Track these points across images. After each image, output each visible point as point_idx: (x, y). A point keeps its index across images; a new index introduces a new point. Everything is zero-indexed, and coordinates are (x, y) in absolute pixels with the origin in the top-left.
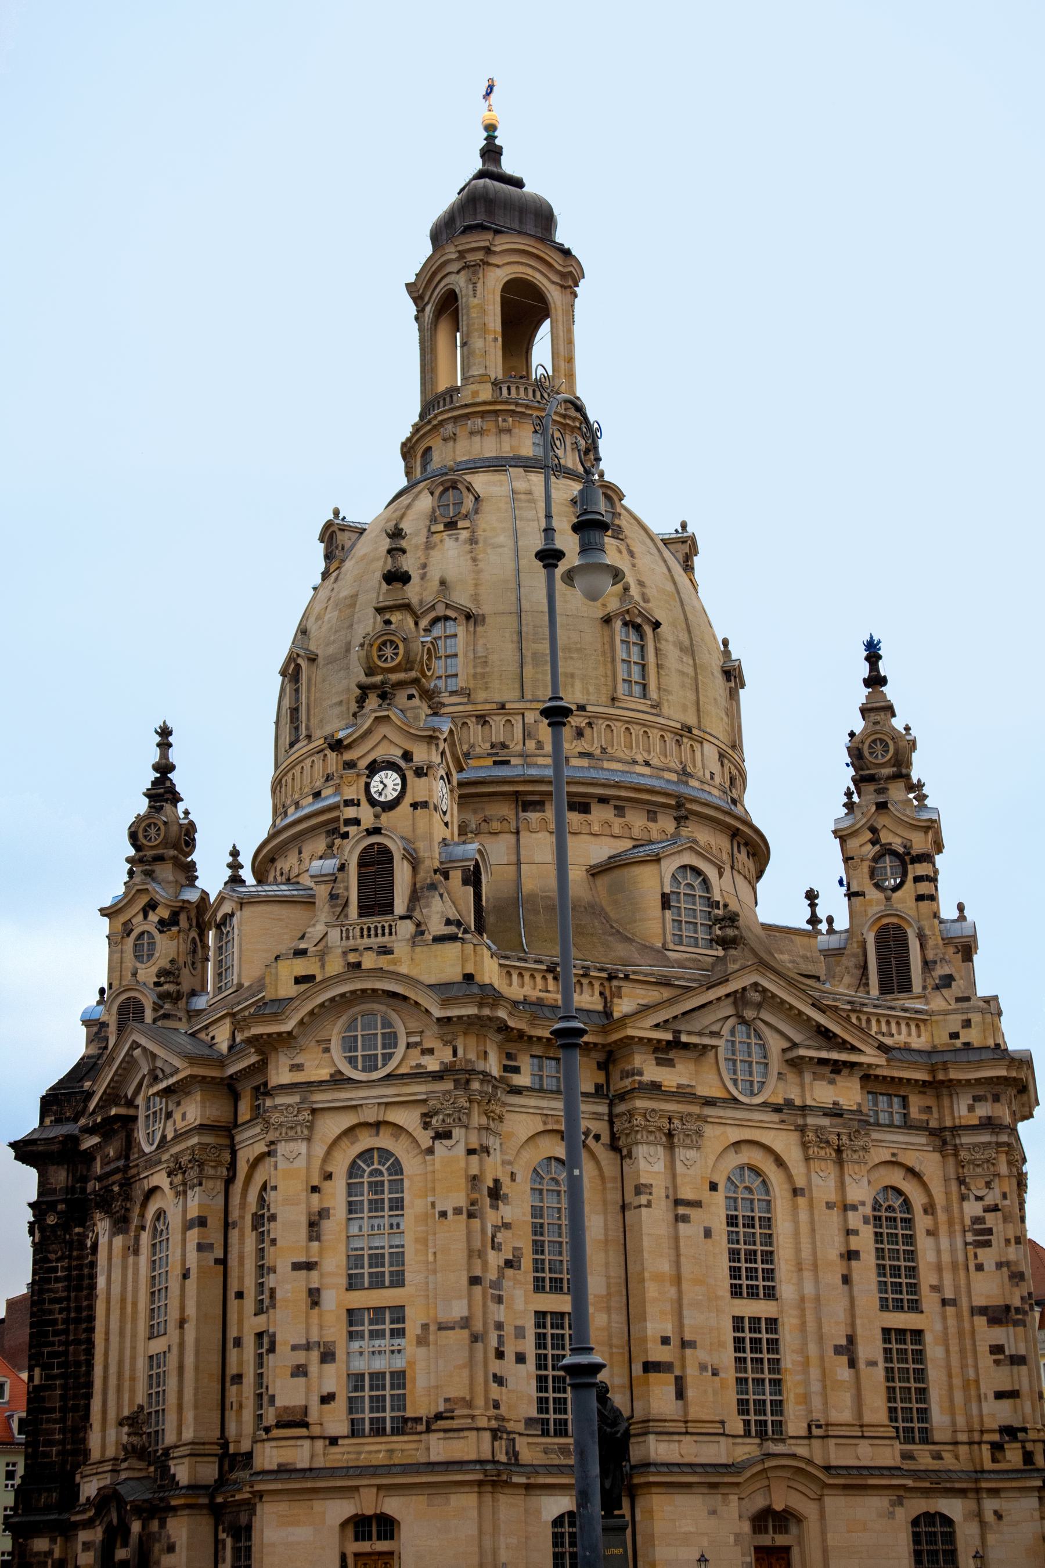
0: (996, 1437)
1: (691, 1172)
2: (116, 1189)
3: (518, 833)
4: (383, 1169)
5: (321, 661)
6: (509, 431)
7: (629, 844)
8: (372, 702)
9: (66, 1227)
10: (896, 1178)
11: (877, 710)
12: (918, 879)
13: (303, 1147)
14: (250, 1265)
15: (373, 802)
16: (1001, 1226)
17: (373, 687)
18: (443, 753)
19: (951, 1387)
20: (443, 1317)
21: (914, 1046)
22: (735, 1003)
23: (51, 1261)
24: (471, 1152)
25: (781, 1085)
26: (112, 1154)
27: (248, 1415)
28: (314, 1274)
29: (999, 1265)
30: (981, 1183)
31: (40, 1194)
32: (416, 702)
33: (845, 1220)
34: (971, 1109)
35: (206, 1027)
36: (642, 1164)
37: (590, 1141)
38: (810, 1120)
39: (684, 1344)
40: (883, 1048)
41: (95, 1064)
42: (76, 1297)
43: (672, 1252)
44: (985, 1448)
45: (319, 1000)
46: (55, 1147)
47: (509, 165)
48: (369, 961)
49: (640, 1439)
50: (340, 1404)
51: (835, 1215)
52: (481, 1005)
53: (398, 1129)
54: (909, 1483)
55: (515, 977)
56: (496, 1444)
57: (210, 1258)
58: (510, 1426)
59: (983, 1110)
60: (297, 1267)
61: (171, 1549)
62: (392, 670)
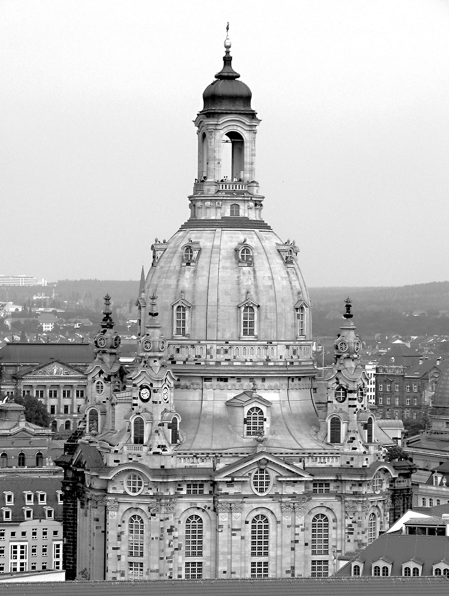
1: (238, 520)
3: (202, 389)
4: (139, 521)
7: (242, 391)
12: (350, 399)
21: (334, 466)
23: (68, 502)
24: (161, 520)
25: (275, 488)
36: (220, 519)
37: (206, 509)
38: (283, 500)
39: (232, 573)
41: (83, 432)
53: (142, 511)
55: (182, 459)
59: (355, 489)
60: (114, 549)
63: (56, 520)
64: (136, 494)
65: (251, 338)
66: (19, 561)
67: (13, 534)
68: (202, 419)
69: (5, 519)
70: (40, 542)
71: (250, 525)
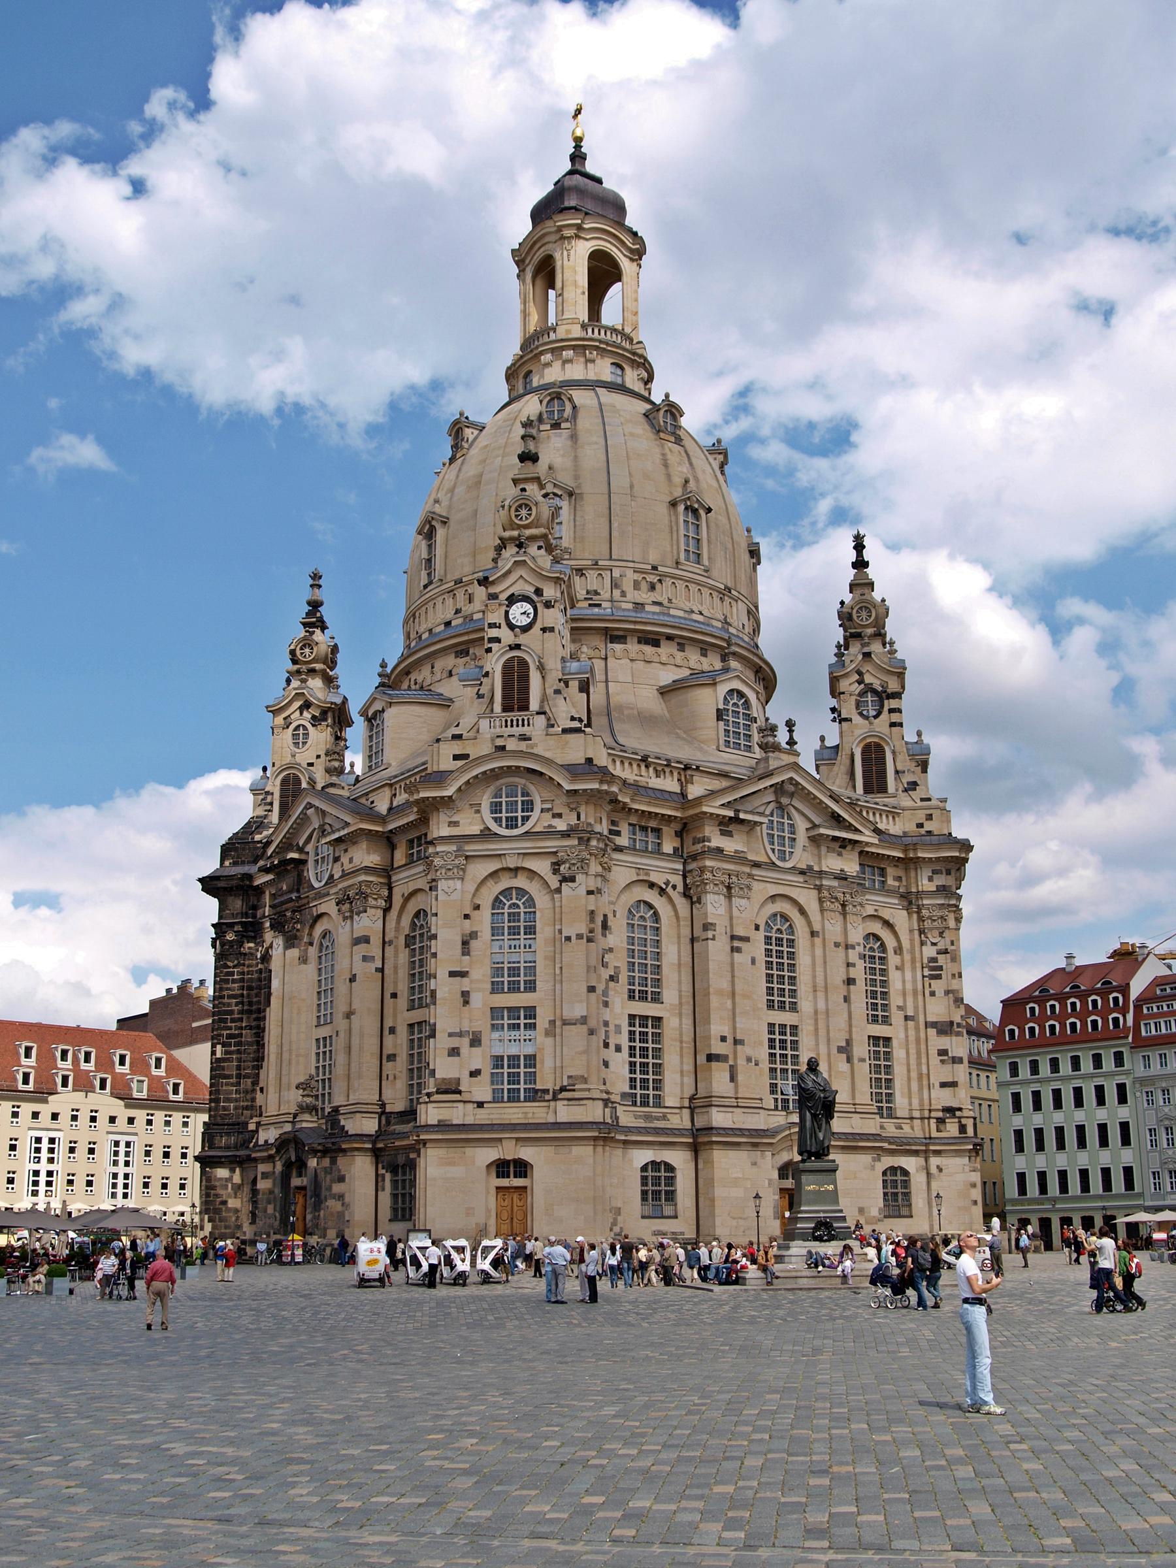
0: (940, 1114)
2: (289, 914)
3: (606, 659)
4: (520, 903)
5: (452, 523)
6: (593, 361)
8: (510, 552)
9: (241, 944)
10: (876, 928)
11: (862, 584)
12: (891, 711)
13: (458, 884)
14: (403, 974)
15: (512, 627)
16: (949, 965)
17: (512, 539)
18: (562, 593)
19: (909, 1079)
20: (567, 1015)
21: (891, 832)
22: (775, 792)
24: (590, 893)
26: (285, 888)
27: (401, 1085)
28: (465, 979)
29: (947, 992)
30: (936, 933)
31: (220, 917)
32: (543, 551)
33: (847, 956)
34: (930, 879)
35: (367, 794)
36: (709, 906)
38: (825, 882)
40: (877, 831)
42: (248, 995)
43: (729, 975)
44: (933, 1121)
45: (474, 773)
46: (234, 883)
47: (590, 167)
48: (512, 745)
49: (704, 1110)
50: (485, 1076)
51: (841, 949)
52: (601, 782)
53: (532, 874)
54: (886, 1145)
55: (618, 763)
56: (607, 1110)
57: (372, 967)
58: (613, 1098)
59: (940, 880)
60: (452, 974)
61: (341, 1179)
62: (526, 527)
63: (112, 1095)
64: (515, 832)
65: (698, 569)
66: (44, 1167)
67: (35, 1115)
68: (614, 714)
69: (21, 1087)
70: (83, 1134)
71: (762, 934)
